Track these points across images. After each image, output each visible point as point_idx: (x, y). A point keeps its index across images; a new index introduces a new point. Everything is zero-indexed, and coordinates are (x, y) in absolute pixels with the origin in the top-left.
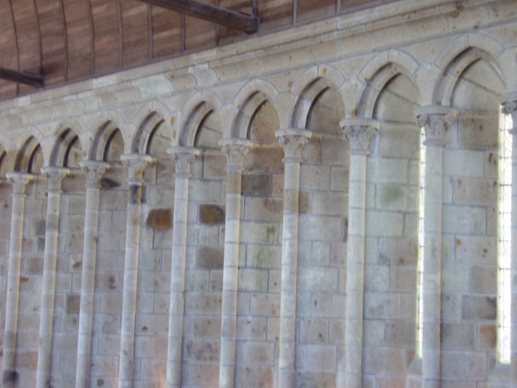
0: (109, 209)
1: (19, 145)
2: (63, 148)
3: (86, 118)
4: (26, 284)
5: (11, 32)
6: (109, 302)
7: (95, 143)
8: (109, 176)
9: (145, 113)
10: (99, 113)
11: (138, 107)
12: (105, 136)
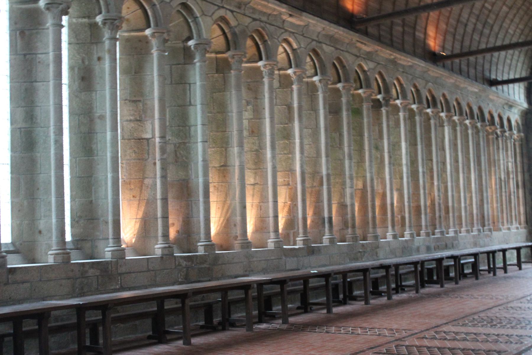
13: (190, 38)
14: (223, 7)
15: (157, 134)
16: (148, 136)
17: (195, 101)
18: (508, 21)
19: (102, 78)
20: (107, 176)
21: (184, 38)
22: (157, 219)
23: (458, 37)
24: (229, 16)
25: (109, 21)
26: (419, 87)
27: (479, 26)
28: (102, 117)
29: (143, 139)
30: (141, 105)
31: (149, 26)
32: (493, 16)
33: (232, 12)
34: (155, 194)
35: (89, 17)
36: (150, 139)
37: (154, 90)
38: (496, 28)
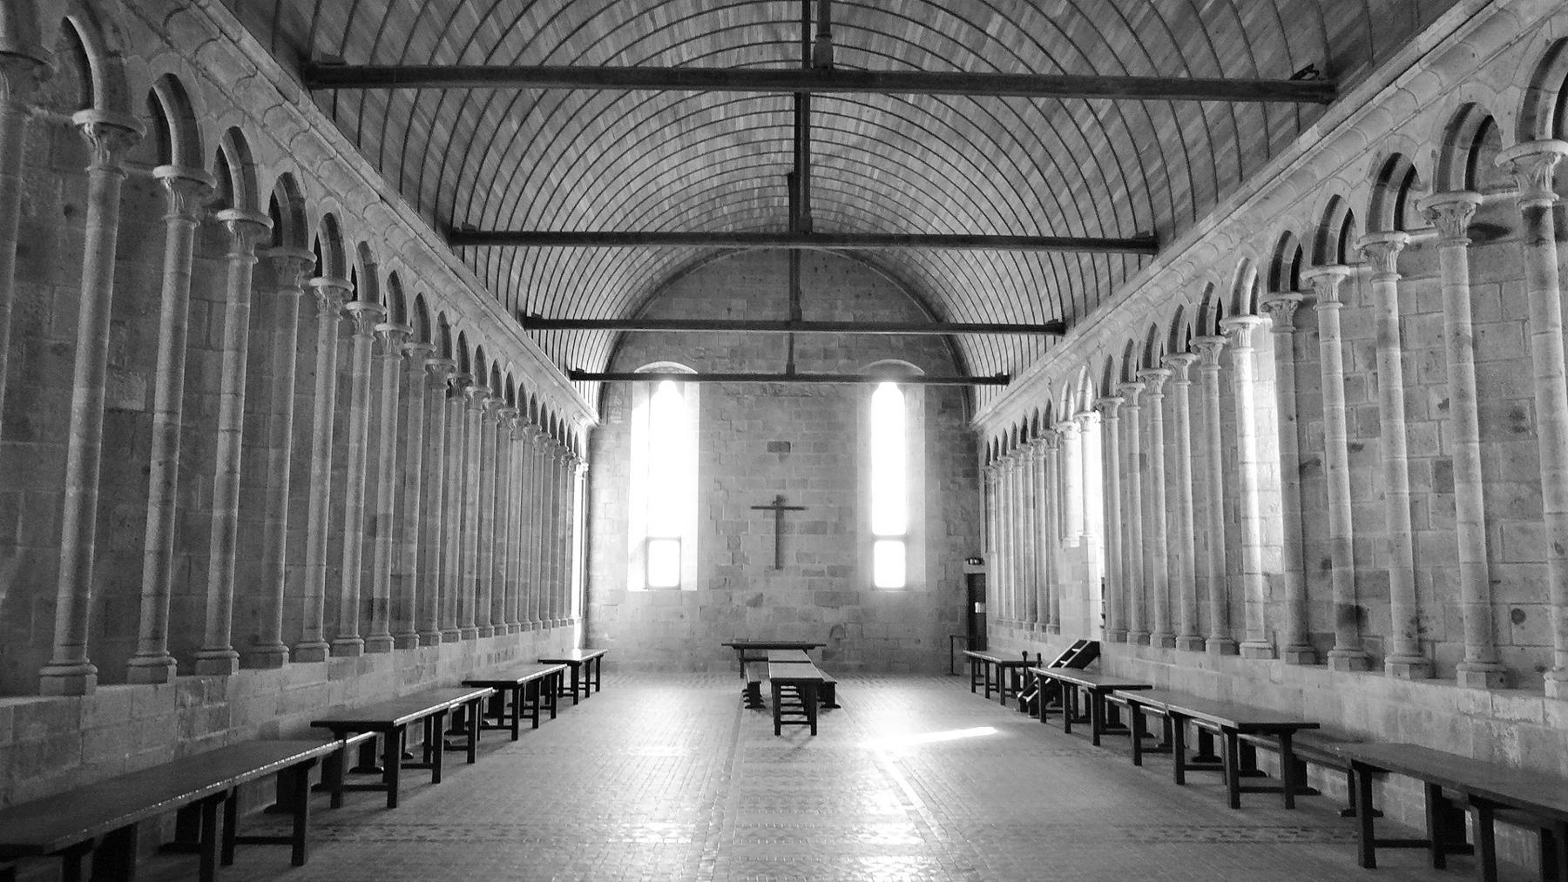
0: (1492, 281)
1: (1316, 221)
2: (1390, 199)
3: (1419, 121)
4: (1361, 454)
5: (1276, 34)
6: (1515, 459)
7: (1445, 159)
8: (1484, 218)
9: (1538, 49)
10: (1444, 99)
11: (1521, 46)
12: (1464, 140)
13: (225, 204)
14: (291, 155)
15: (160, 401)
16: (138, 405)
17: (220, 339)
18: (606, 277)
19: (76, 257)
20: (64, 494)
21: (210, 199)
22: (139, 600)
23: (552, 290)
24: (297, 176)
25: (112, 131)
26: (501, 367)
27: (576, 278)
28: (65, 352)
29: (120, 411)
30: (123, 333)
31: (165, 160)
32: (593, 265)
33: (302, 168)
34: (141, 540)
35: (53, 106)
36: (140, 412)
37: (158, 305)
38: (591, 285)
